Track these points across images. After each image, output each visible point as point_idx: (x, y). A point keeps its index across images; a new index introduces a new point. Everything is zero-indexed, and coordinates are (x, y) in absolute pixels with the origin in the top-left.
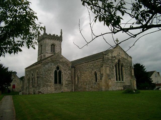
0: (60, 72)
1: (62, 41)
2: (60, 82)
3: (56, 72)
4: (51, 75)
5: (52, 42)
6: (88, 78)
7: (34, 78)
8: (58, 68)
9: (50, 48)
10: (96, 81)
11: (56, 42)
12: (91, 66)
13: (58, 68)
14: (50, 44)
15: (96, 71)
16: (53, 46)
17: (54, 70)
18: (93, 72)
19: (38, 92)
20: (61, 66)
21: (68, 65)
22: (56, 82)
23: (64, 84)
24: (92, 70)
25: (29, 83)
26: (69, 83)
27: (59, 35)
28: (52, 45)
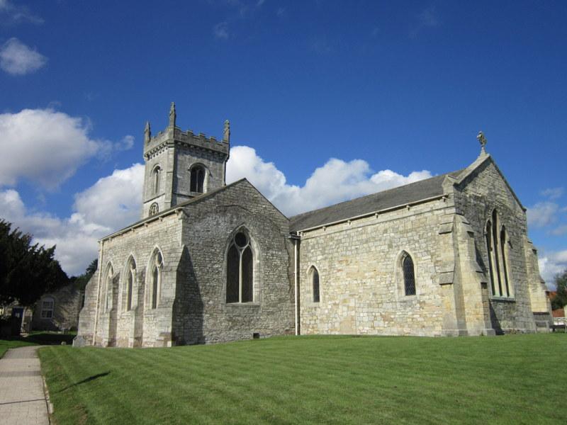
0: (249, 255)
1: (228, 158)
2: (247, 296)
6: (369, 282)
7: (142, 276)
10: (410, 288)
12: (385, 231)
14: (189, 166)
15: (408, 251)
16: (198, 172)
18: (395, 256)
24: (390, 246)
25: (115, 294)
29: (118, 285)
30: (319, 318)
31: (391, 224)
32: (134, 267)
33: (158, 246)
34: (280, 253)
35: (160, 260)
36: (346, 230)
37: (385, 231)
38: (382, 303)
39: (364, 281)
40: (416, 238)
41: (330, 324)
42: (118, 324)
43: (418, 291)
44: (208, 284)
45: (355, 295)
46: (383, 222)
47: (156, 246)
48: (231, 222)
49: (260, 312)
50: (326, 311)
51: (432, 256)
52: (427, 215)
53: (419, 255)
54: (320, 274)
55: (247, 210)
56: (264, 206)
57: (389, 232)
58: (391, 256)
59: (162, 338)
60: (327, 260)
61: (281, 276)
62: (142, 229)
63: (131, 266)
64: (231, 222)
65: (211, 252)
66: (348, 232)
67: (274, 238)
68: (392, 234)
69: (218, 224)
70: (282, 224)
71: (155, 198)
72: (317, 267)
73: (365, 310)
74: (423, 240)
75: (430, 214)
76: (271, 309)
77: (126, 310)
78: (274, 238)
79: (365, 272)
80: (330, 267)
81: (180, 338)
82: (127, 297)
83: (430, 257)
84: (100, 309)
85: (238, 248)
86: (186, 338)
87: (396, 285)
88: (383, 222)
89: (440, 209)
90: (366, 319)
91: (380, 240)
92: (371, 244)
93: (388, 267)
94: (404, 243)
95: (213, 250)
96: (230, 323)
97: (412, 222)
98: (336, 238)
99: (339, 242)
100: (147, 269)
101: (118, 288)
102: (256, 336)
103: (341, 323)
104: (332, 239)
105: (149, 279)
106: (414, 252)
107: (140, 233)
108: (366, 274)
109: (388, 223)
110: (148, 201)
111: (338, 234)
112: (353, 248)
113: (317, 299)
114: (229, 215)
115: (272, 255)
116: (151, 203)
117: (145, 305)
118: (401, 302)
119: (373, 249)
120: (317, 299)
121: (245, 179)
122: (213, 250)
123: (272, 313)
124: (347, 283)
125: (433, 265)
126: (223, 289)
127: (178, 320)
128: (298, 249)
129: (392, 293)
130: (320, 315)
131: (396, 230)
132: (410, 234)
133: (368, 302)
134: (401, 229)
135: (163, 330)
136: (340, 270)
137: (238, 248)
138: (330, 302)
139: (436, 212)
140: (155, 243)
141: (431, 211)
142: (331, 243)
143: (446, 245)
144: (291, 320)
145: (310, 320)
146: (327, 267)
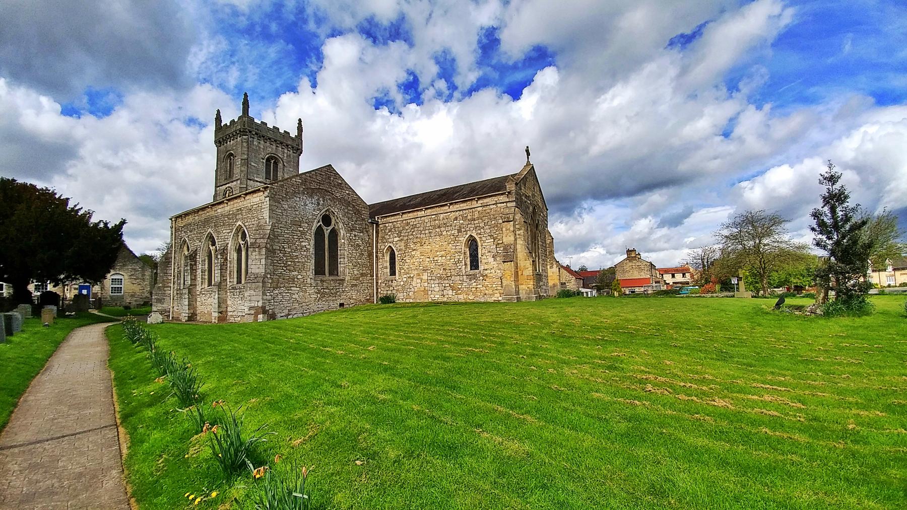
0: (334, 234)
1: (301, 153)
2: (334, 270)
3: (319, 233)
4: (303, 244)
5: (271, 149)
7: (224, 251)
8: (326, 220)
9: (262, 167)
11: (283, 153)
12: (456, 219)
13: (326, 220)
15: (474, 235)
16: (272, 161)
17: (315, 226)
18: (463, 239)
19: (251, 308)
20: (338, 212)
21: (358, 212)
22: (319, 270)
23: (347, 278)
24: (459, 231)
25: (193, 270)
26: (362, 275)
27: (294, 133)
28: (268, 160)
29: (196, 262)
30: (395, 288)
31: (461, 213)
32: (214, 244)
33: (241, 224)
34: (361, 234)
35: (244, 236)
36: (421, 217)
37: (456, 219)
38: (451, 276)
39: (436, 259)
40: (482, 225)
41: (405, 294)
42: (198, 299)
43: (481, 267)
44: (297, 260)
45: (428, 270)
46: (454, 211)
47: (239, 223)
48: (318, 204)
49: (345, 285)
50: (402, 283)
51: (494, 240)
52: (492, 207)
53: (484, 239)
54: (396, 253)
55: (332, 194)
56: (347, 192)
57: (458, 219)
58: (460, 239)
59: (253, 312)
60: (404, 241)
61: (363, 254)
62: (222, 206)
63: (210, 243)
64: (318, 204)
65: (300, 231)
66: (423, 218)
67: (356, 221)
68: (461, 222)
69: (305, 205)
70: (363, 209)
71: (228, 183)
72: (393, 247)
73: (437, 282)
74: (487, 227)
75: (494, 206)
76: (355, 282)
77: (206, 286)
78: (356, 221)
79: (437, 251)
80: (406, 246)
81: (270, 311)
82: (207, 273)
83: (493, 240)
84: (176, 286)
85: (324, 228)
86: (276, 311)
87: (463, 262)
88: (454, 211)
89: (503, 203)
90: (437, 289)
91: (451, 226)
92: (442, 229)
93: (457, 247)
94: (472, 229)
95: (302, 229)
96: (319, 295)
97: (479, 212)
98: (412, 223)
99: (414, 226)
100: (229, 245)
101: (196, 265)
102: (342, 305)
103: (414, 292)
104: (408, 224)
105: (233, 256)
106: (479, 236)
107: (219, 211)
108: (438, 253)
109: (458, 212)
110: (224, 185)
111: (413, 220)
112: (427, 232)
113: (393, 273)
114: (316, 198)
115: (355, 236)
116: (224, 187)
117: (228, 280)
118: (467, 275)
119: (444, 233)
120: (393, 273)
121: (330, 165)
122: (302, 229)
123: (356, 285)
124: (421, 260)
125: (495, 247)
126: (311, 265)
127: (268, 294)
128: (377, 232)
129: (460, 269)
130: (396, 286)
131: (465, 218)
132: (477, 222)
133: (439, 275)
134: (469, 217)
135: (253, 305)
136: (415, 250)
137: (324, 228)
138: (405, 276)
139: (499, 205)
140: (237, 221)
141: (496, 204)
142: (407, 228)
143: (508, 231)
144: (370, 291)
145: (387, 291)
146: (403, 247)
